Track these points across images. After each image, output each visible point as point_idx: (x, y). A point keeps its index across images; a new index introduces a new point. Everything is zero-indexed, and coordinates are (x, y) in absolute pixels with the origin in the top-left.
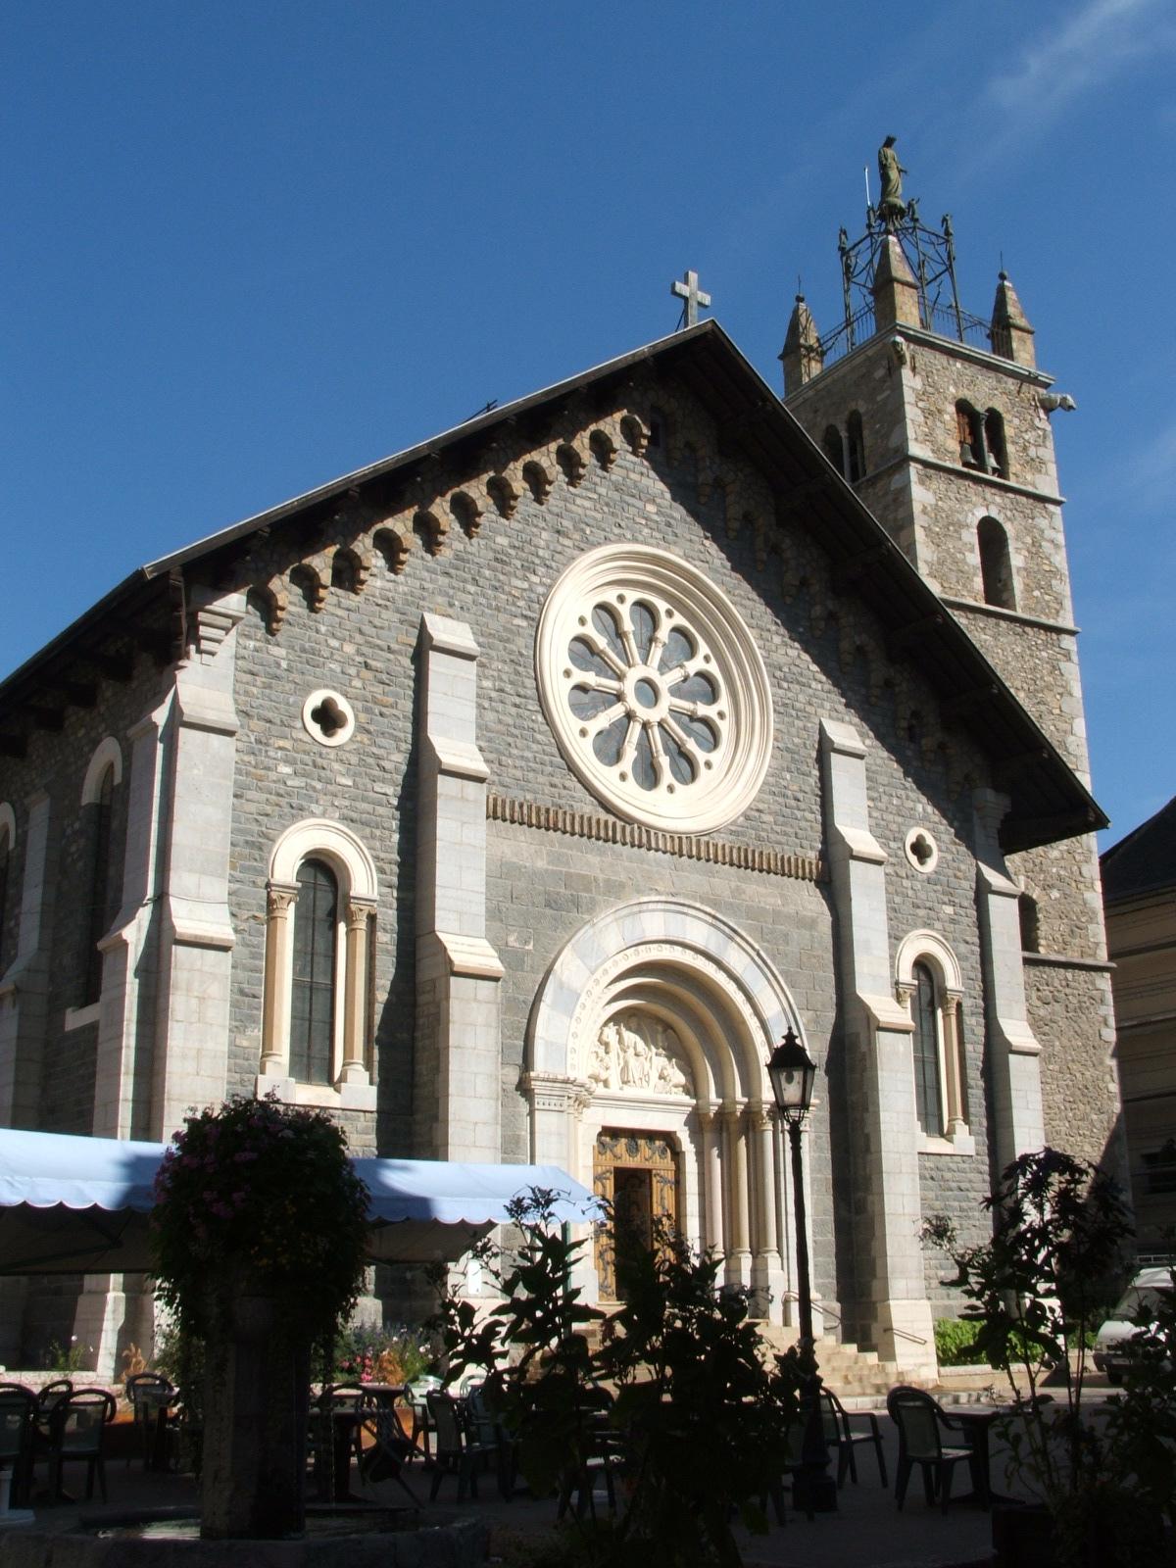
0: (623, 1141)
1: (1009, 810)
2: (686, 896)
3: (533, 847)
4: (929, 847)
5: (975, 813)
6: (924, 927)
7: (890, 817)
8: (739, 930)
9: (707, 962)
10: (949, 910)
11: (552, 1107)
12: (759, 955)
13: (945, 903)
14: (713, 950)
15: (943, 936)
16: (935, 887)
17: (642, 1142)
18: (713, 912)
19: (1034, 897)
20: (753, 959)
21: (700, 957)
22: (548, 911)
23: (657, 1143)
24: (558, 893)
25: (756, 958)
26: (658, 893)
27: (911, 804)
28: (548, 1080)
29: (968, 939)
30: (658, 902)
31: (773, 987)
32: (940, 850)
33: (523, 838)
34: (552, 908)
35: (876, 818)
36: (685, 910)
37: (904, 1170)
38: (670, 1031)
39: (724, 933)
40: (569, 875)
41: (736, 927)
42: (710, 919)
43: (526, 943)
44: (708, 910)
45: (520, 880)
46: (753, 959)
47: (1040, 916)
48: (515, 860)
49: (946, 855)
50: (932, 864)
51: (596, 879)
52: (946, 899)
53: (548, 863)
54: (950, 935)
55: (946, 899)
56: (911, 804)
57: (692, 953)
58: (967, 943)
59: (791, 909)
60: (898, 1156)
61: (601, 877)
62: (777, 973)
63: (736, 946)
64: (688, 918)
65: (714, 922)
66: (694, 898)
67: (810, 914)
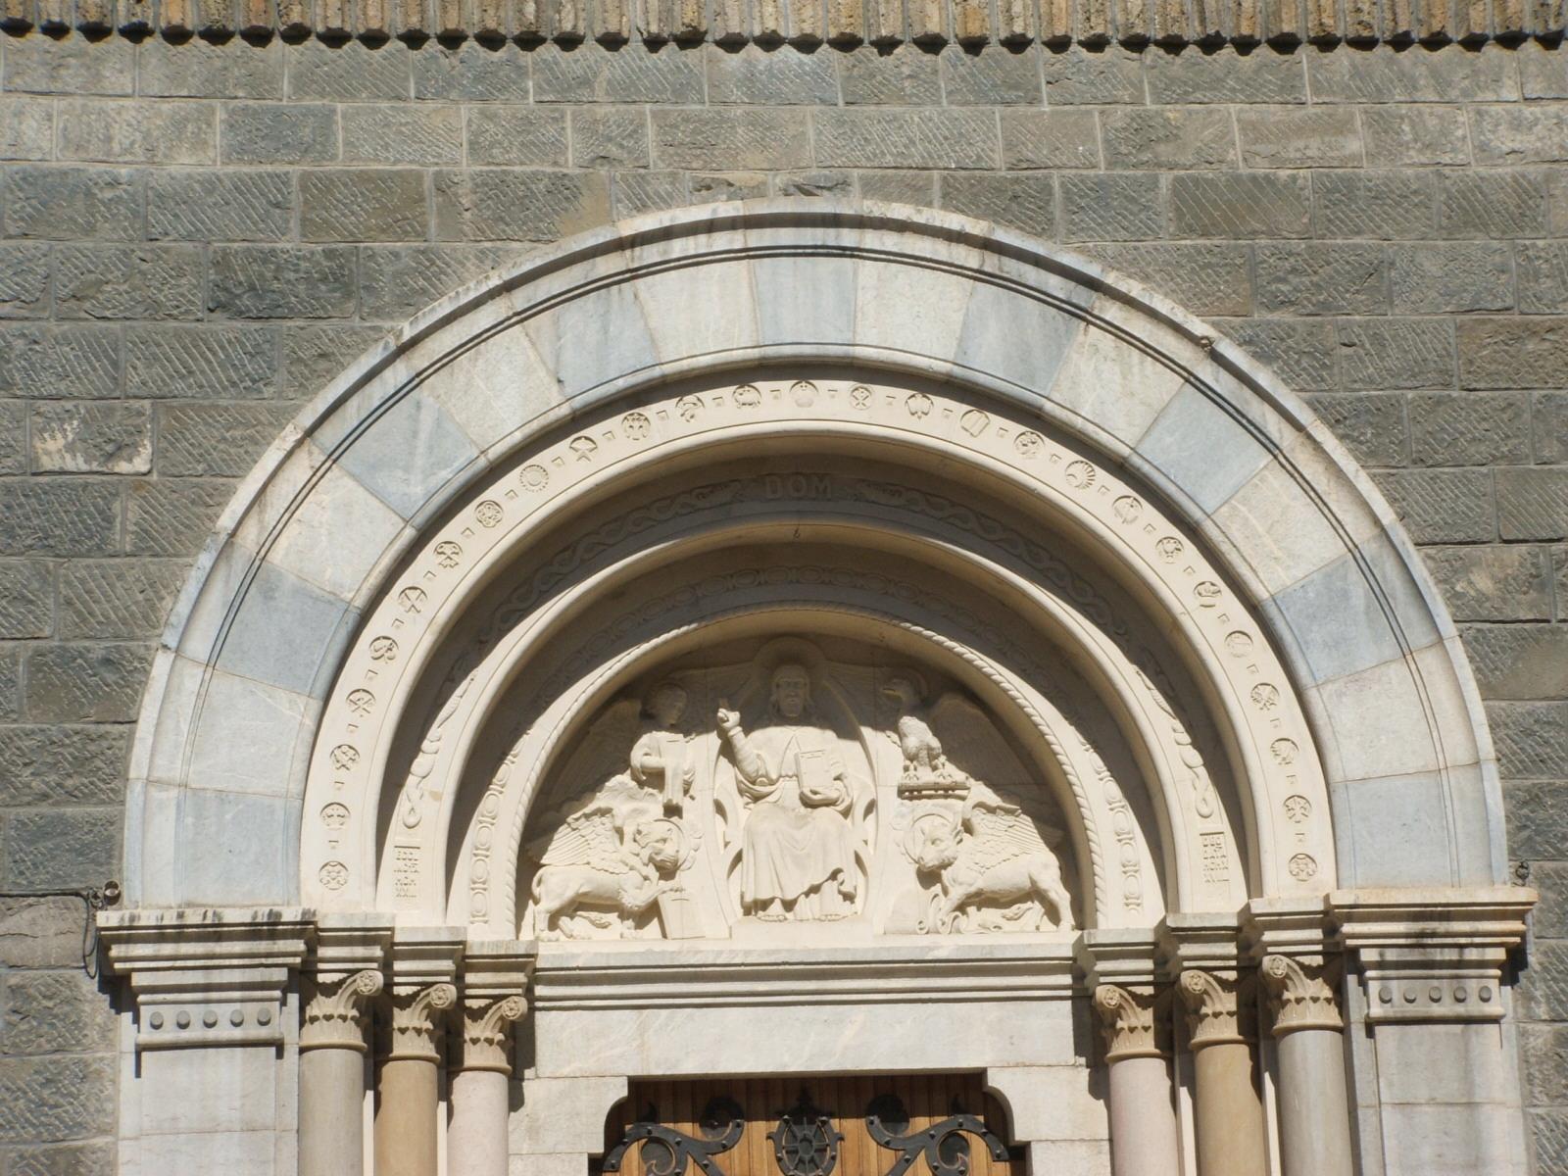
0: (758, 1130)
2: (870, 188)
3: (166, 107)
8: (1111, 279)
9: (920, 402)
11: (224, 1032)
12: (1217, 358)
14: (990, 368)
17: (851, 1129)
18: (976, 227)
20: (1191, 379)
21: (941, 403)
22: (223, 326)
23: (921, 1124)
24: (267, 257)
25: (1207, 372)
26: (733, 191)
28: (180, 933)
30: (711, 227)
31: (1294, 473)
33: (126, 83)
34: (240, 314)
36: (848, 237)
38: (950, 703)
39: (1043, 297)
40: (319, 188)
41: (1093, 270)
42: (970, 257)
43: (123, 448)
44: (954, 221)
45: (90, 230)
46: (1191, 379)
48: (69, 162)
51: (444, 186)
53: (228, 159)
57: (727, 392)
59: (1411, 165)
61: (467, 167)
62: (1305, 416)
63: (1107, 341)
64: (868, 269)
65: (992, 263)
66: (918, 194)
67: (1506, 170)
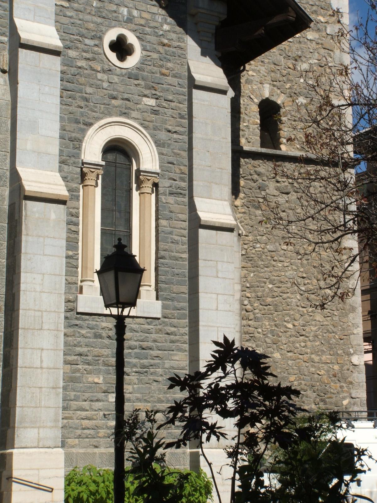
1: (224, 17)
4: (131, 45)
5: (189, 19)
6: (120, 115)
7: (88, 17)
10: (152, 102)
13: (145, 96)
15: (141, 124)
16: (136, 82)
19: (279, 102)
27: (114, 8)
29: (170, 128)
32: (144, 49)
35: (71, 17)
37: (46, 326)
47: (284, 119)
49: (149, 54)
50: (132, 61)
52: (147, 92)
54: (151, 125)
55: (147, 92)
56: (114, 8)
58: (169, 131)
60: (38, 314)
